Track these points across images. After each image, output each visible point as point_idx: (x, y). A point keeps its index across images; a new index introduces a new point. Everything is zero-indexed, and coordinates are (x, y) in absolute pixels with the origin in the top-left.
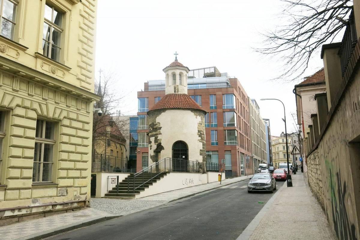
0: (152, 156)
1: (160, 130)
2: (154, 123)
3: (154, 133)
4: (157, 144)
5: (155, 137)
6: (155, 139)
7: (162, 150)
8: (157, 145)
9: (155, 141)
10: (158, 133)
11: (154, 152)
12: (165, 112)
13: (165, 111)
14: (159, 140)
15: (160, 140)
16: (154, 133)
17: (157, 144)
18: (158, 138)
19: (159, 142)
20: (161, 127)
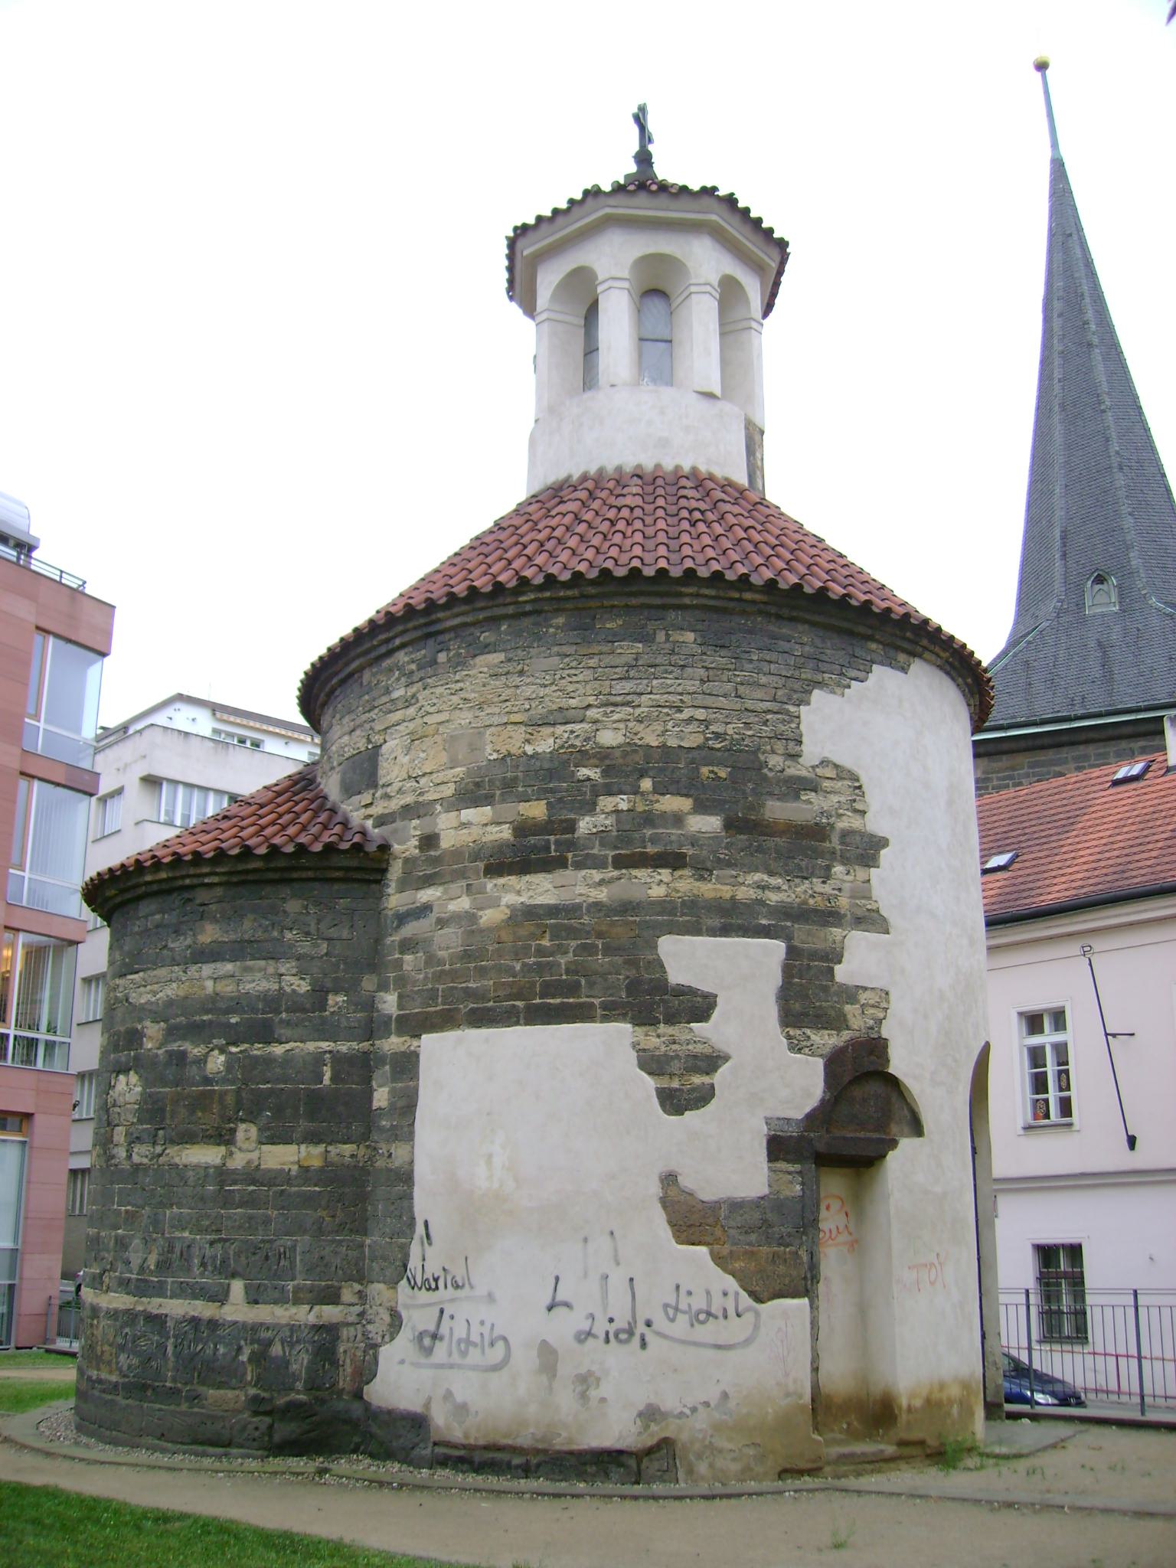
0: (736, 1206)
1: (861, 873)
2: (775, 761)
3: (782, 892)
4: (827, 1040)
5: (792, 952)
6: (788, 970)
7: (907, 1145)
8: (834, 1063)
9: (785, 995)
10: (844, 903)
11: (779, 1147)
12: (904, 670)
13: (902, 657)
14: (851, 994)
15: (863, 997)
16: (782, 892)
17: (827, 1040)
18: (843, 973)
19: (857, 1021)
20: (883, 843)
